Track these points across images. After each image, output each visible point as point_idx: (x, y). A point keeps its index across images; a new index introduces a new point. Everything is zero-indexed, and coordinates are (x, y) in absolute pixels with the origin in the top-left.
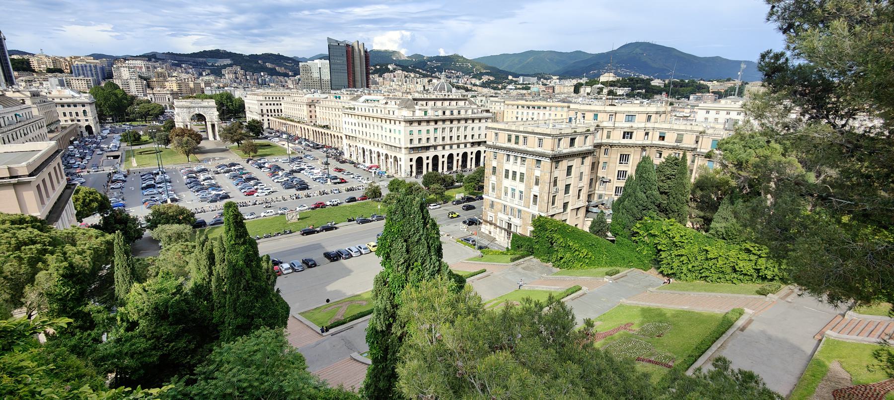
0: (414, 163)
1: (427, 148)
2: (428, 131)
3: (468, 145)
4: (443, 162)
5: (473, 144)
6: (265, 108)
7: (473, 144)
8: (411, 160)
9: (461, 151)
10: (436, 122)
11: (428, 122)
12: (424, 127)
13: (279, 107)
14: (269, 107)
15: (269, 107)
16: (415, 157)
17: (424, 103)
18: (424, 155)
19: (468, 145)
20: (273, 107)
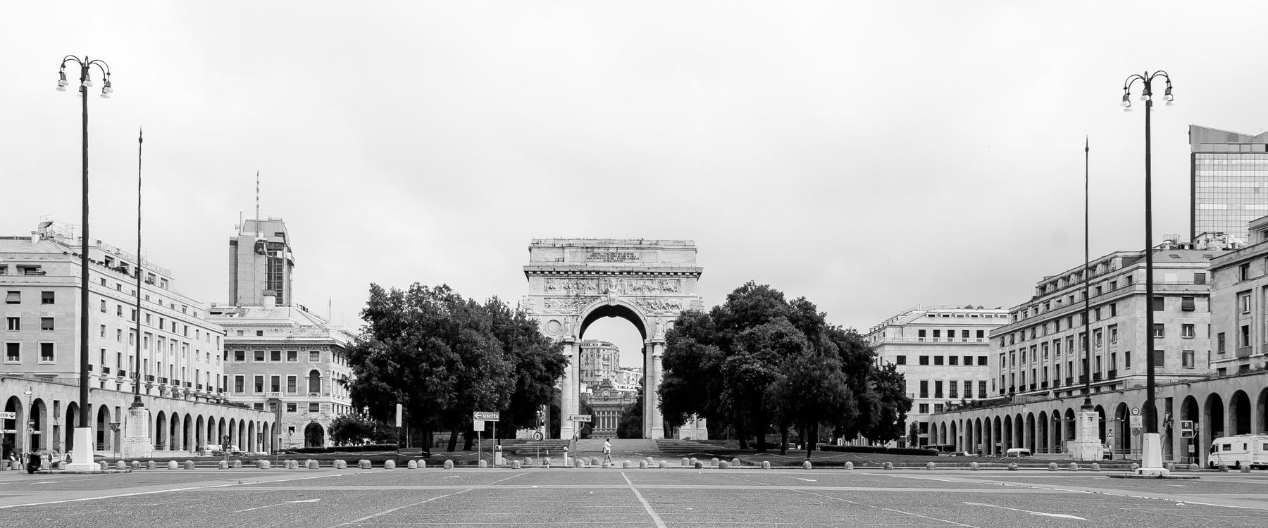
14: (933, 373)
15: (933, 373)
20: (946, 373)
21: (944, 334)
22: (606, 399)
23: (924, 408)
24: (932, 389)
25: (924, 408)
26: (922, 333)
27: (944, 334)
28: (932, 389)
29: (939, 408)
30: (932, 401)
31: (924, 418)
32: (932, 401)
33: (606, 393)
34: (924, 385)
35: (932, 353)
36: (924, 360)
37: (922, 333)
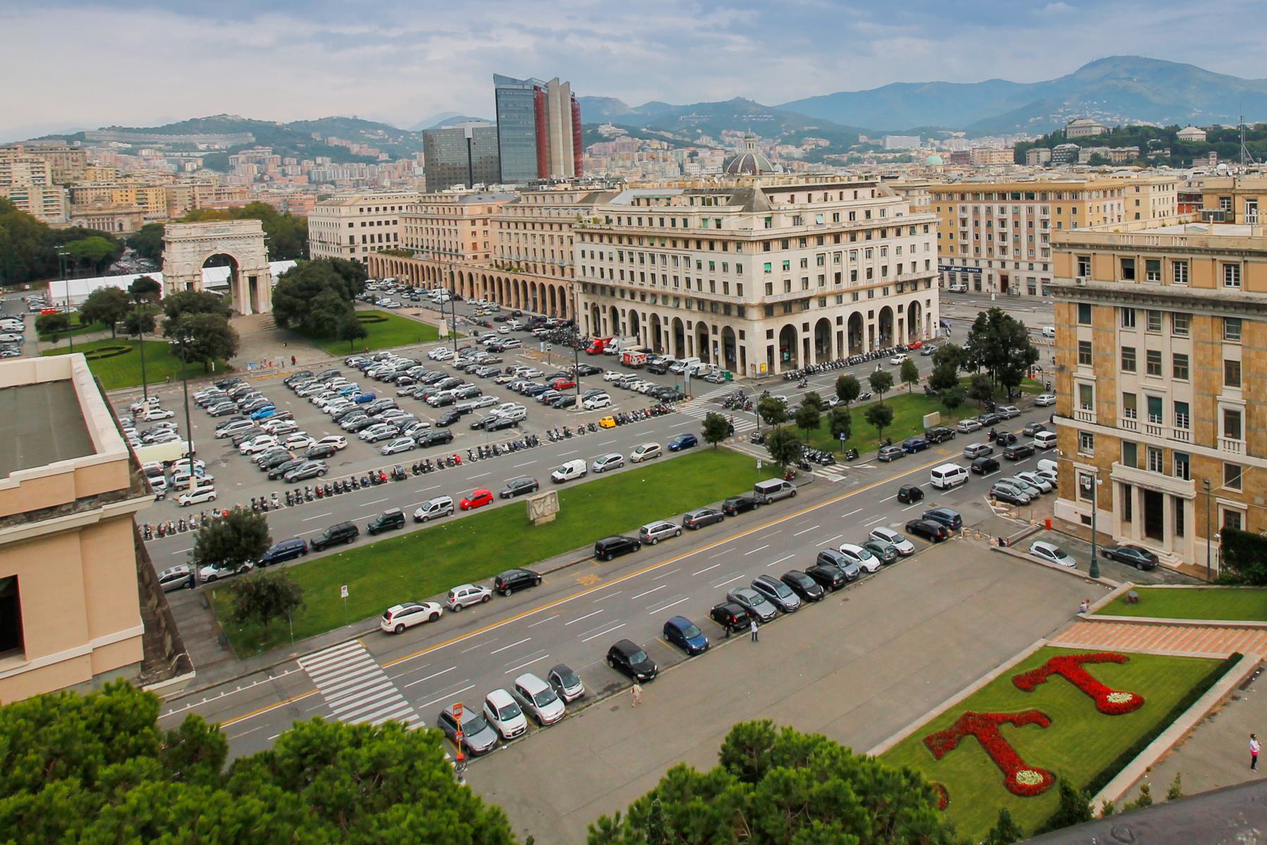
0: (776, 342)
1: (804, 303)
2: (804, 263)
3: (892, 290)
4: (840, 334)
5: (901, 287)
6: (358, 232)
7: (901, 287)
8: (770, 334)
9: (877, 305)
10: (820, 239)
11: (803, 240)
12: (794, 254)
13: (391, 229)
14: (368, 231)
15: (368, 231)
16: (777, 325)
17: (787, 196)
18: (797, 321)
19: (892, 290)
20: (376, 230)
21: (373, 210)
22: (100, 209)
23: (365, 249)
24: (368, 239)
25: (365, 249)
26: (361, 210)
27: (373, 210)
28: (368, 239)
29: (373, 248)
30: (369, 245)
31: (366, 254)
32: (369, 245)
33: (100, 205)
34: (364, 237)
35: (367, 220)
36: (363, 224)
37: (361, 210)
